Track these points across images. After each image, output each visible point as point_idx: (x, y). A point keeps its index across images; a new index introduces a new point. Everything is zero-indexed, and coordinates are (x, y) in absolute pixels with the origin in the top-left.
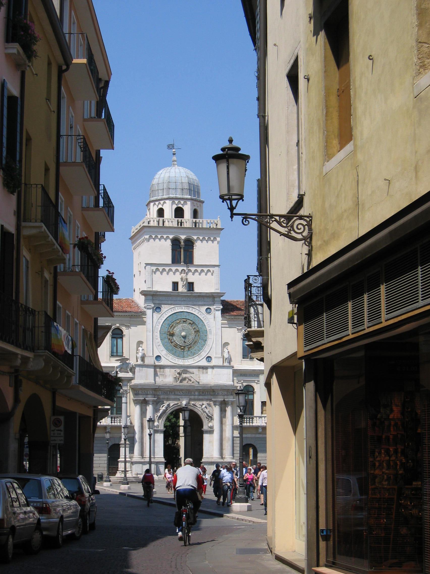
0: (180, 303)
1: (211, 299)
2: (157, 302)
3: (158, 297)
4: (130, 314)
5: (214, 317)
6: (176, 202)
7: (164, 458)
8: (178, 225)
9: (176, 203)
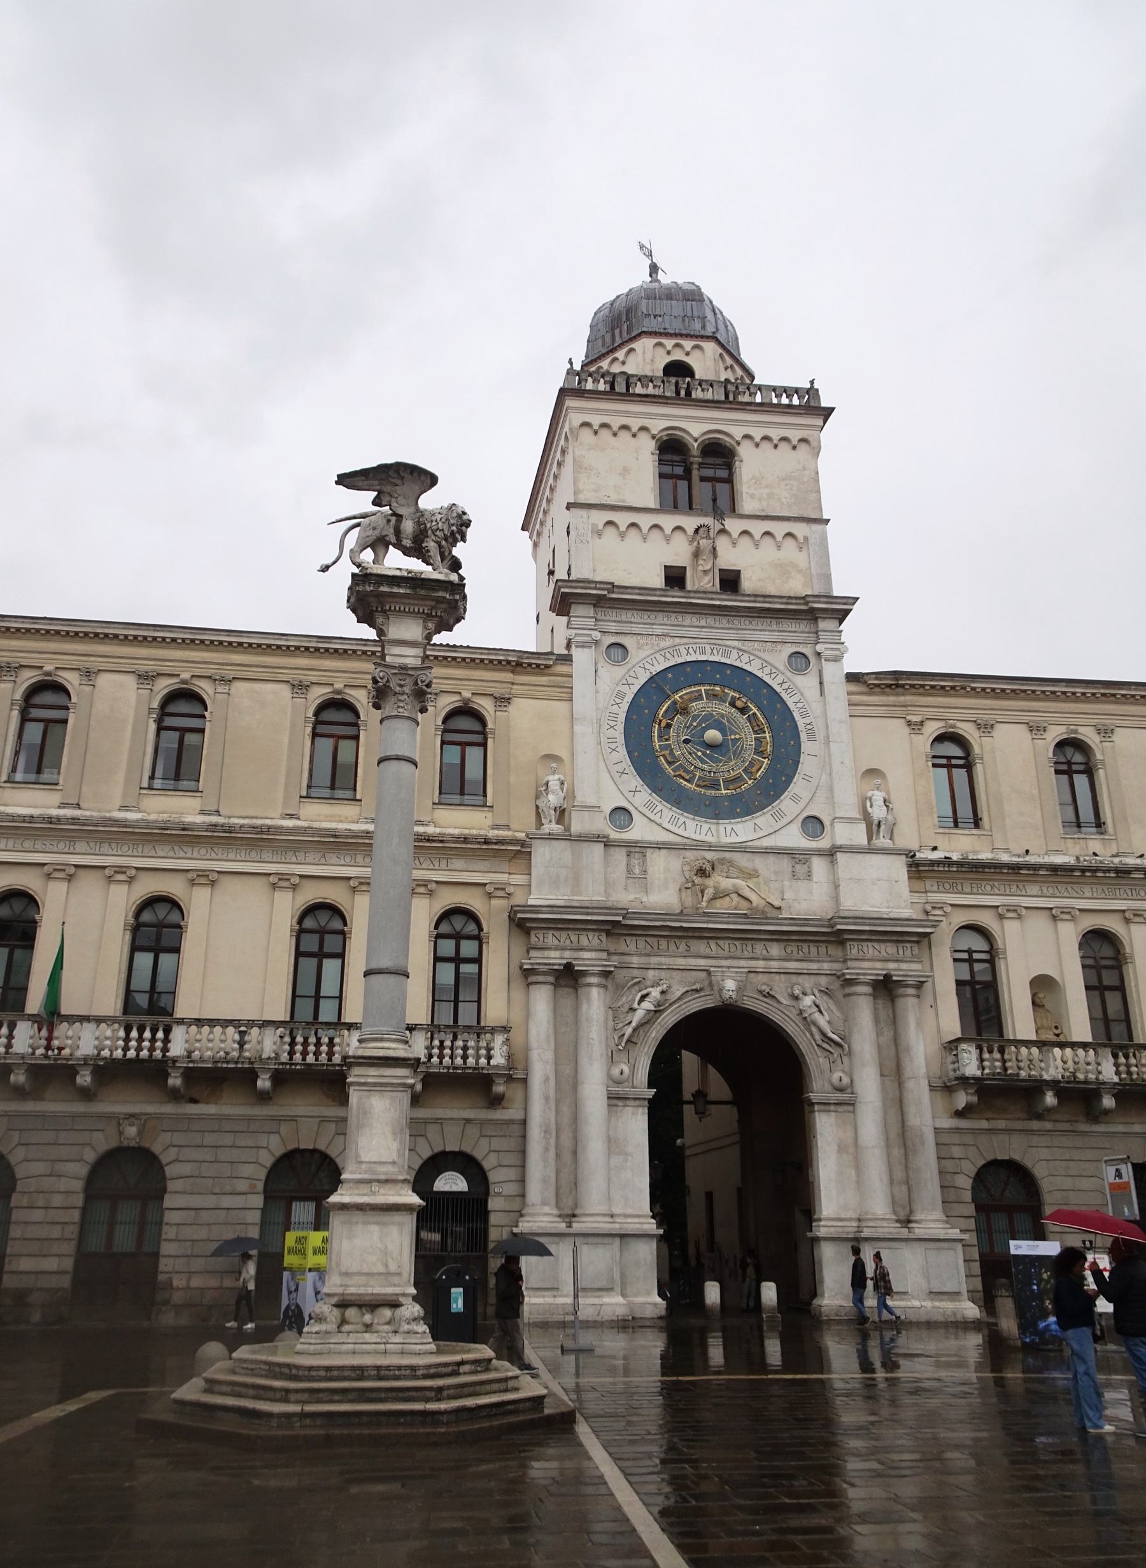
1: (804, 626)
2: (613, 627)
3: (614, 611)
5: (821, 683)
6: (669, 343)
7: (653, 1217)
8: (678, 393)
9: (669, 348)
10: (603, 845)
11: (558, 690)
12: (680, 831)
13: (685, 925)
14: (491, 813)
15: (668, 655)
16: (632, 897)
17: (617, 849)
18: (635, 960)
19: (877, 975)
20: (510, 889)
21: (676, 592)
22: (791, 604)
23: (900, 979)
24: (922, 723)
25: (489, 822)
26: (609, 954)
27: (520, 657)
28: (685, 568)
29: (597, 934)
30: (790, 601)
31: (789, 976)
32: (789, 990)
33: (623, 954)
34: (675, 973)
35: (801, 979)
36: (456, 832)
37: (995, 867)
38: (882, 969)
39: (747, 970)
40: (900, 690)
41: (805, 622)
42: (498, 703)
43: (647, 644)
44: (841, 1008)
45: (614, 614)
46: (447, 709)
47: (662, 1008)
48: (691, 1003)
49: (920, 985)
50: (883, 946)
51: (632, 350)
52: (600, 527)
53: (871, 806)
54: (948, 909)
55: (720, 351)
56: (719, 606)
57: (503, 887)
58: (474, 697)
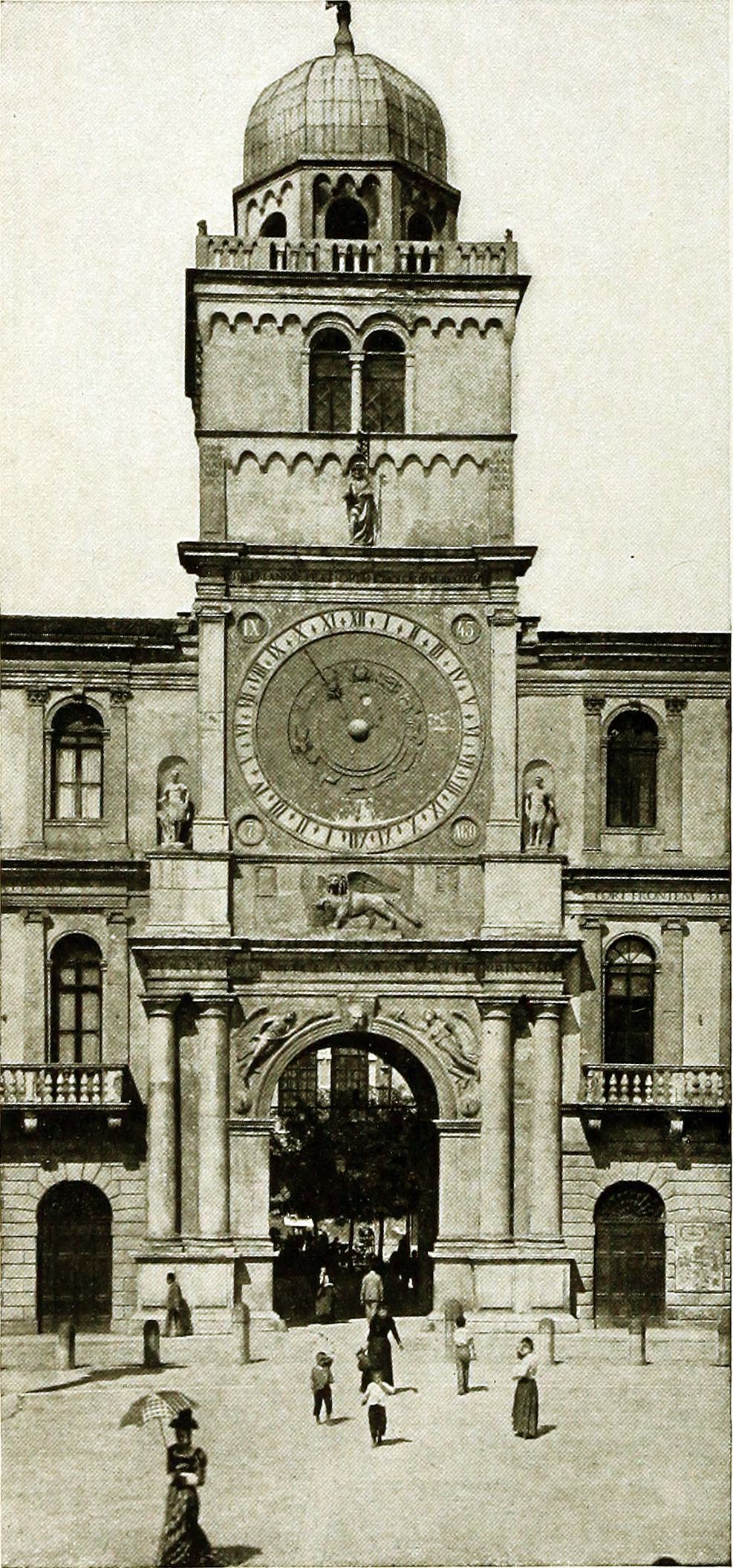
39: (376, 995)
47: (286, 1035)
53: (530, 808)
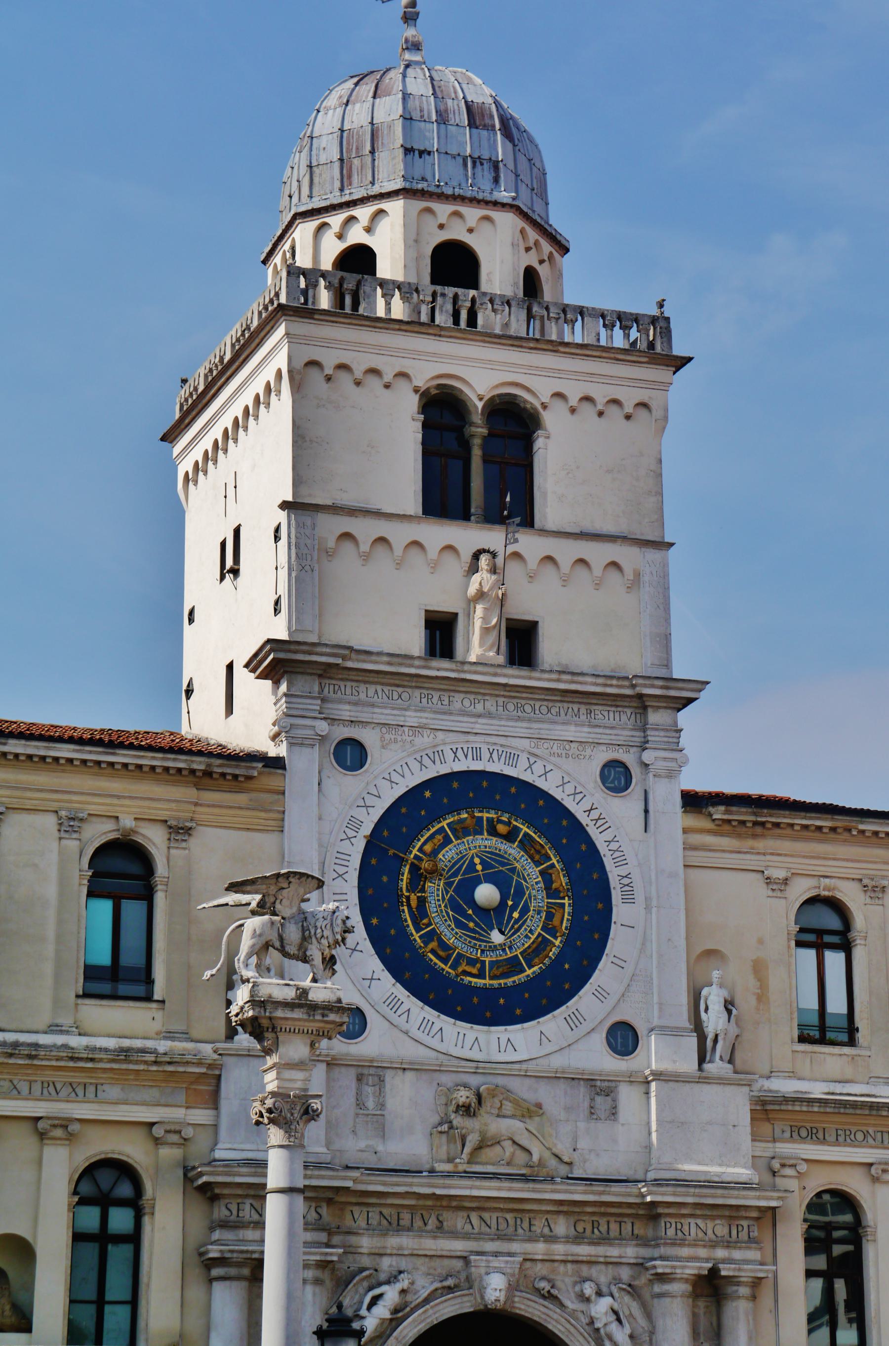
0: (465, 727)
1: (626, 717)
3: (349, 684)
4: (199, 764)
5: (646, 811)
6: (443, 210)
8: (456, 322)
9: (442, 219)
10: (322, 1067)
11: (263, 815)
12: (435, 1043)
13: (438, 1192)
14: (161, 1013)
15: (426, 761)
16: (362, 1144)
17: (343, 1069)
18: (366, 1243)
19: (700, 1268)
20: (188, 1132)
21: (445, 664)
22: (611, 686)
23: (731, 1274)
24: (786, 881)
25: (157, 1026)
26: (330, 1234)
27: (209, 765)
28: (456, 614)
29: (314, 1205)
30: (609, 682)
31: (578, 1265)
32: (577, 1288)
33: (349, 1233)
34: (419, 1262)
35: (594, 1271)
36: (111, 1043)
37: (873, 1106)
38: (707, 1260)
40: (759, 830)
41: (629, 711)
42: (173, 835)
43: (396, 741)
44: (649, 1315)
45: (348, 691)
46: (97, 844)
48: (441, 1306)
49: (756, 1283)
50: (710, 1224)
51: (381, 212)
52: (331, 543)
54: (803, 1167)
55: (520, 223)
56: (505, 685)
57: (177, 1128)
58: (141, 824)
